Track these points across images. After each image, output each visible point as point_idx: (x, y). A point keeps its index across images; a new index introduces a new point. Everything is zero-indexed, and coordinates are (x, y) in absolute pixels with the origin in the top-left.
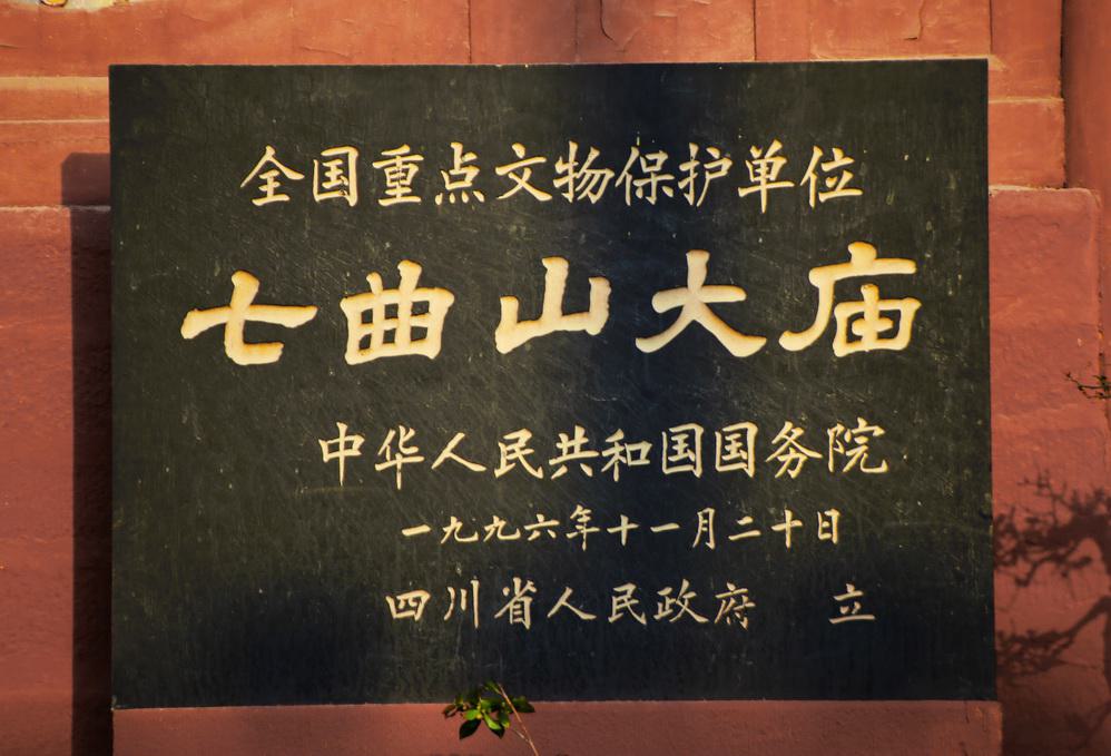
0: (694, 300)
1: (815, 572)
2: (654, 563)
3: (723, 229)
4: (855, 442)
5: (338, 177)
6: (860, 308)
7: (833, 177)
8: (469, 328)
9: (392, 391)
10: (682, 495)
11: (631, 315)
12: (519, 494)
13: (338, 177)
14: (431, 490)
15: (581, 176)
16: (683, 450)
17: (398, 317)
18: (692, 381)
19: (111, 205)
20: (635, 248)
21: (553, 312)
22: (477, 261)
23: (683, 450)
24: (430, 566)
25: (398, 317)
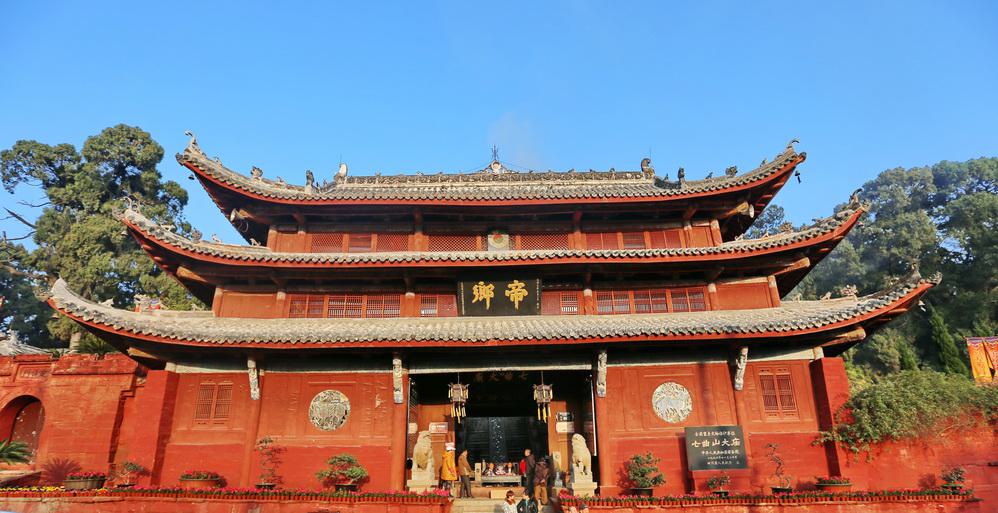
0: (725, 442)
1: (734, 461)
2: (725, 460)
3: (726, 437)
4: (737, 451)
5: (701, 434)
6: (736, 442)
7: (733, 433)
8: (711, 444)
9: (706, 449)
10: (726, 455)
11: (721, 443)
12: (715, 456)
13: (701, 434)
14: (710, 455)
15: (717, 434)
16: (726, 452)
17: (706, 444)
18: (726, 448)
19: (828, 290)
20: (721, 438)
21: (716, 443)
22: (711, 439)
23: (726, 452)
24: (710, 460)
25: (706, 444)
